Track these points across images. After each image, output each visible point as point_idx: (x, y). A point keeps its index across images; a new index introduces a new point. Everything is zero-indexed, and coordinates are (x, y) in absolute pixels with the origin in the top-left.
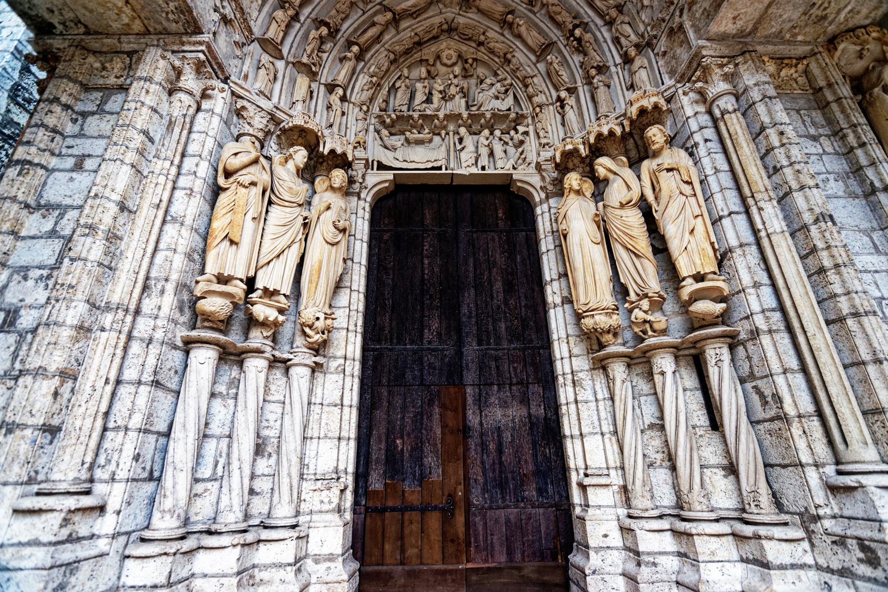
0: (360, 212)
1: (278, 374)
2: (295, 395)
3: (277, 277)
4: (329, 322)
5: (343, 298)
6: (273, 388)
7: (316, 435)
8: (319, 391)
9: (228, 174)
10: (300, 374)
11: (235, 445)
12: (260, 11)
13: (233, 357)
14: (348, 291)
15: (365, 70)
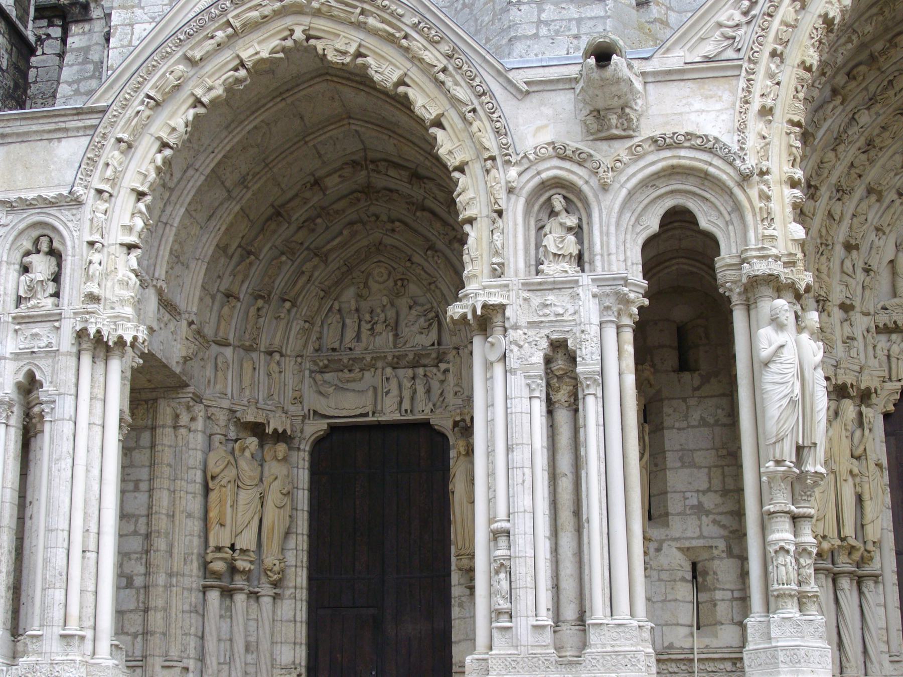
0: (301, 462)
1: (252, 602)
2: (265, 615)
3: (247, 541)
4: (282, 565)
5: (291, 543)
6: (250, 611)
7: (279, 640)
8: (279, 613)
9: (213, 478)
10: (266, 601)
11: (235, 645)
12: (211, 311)
13: (228, 593)
14: (294, 536)
15: (298, 316)
